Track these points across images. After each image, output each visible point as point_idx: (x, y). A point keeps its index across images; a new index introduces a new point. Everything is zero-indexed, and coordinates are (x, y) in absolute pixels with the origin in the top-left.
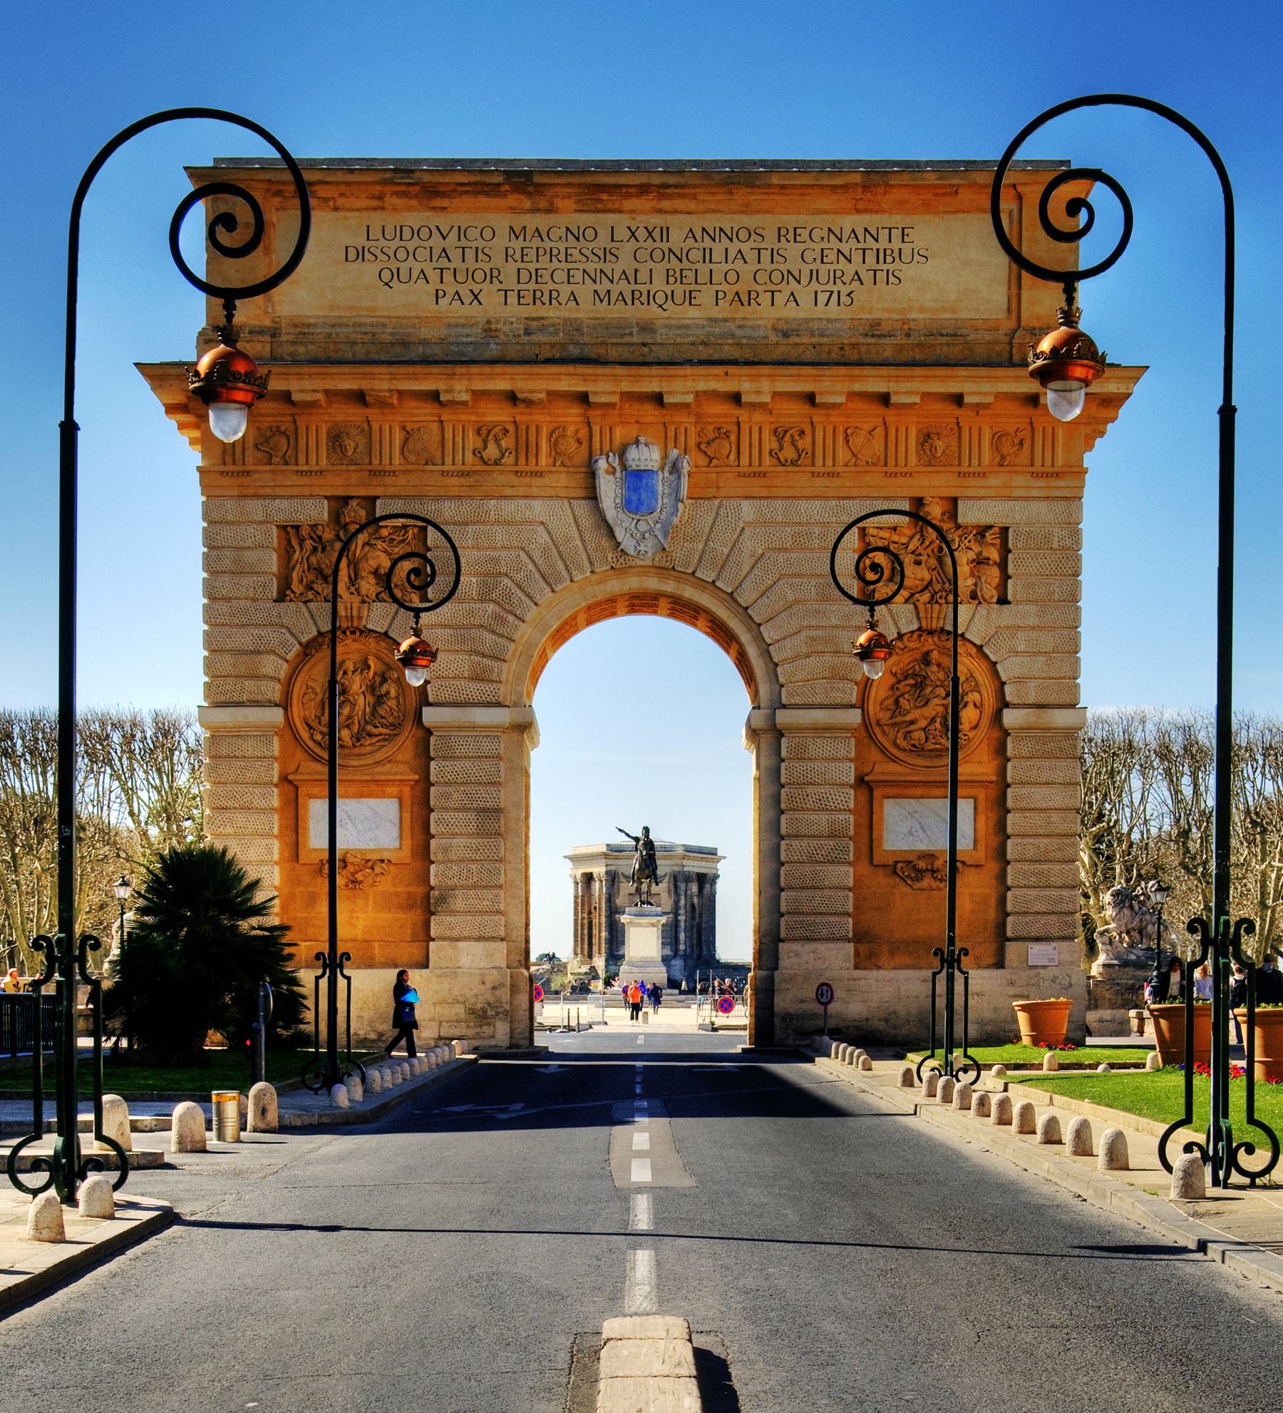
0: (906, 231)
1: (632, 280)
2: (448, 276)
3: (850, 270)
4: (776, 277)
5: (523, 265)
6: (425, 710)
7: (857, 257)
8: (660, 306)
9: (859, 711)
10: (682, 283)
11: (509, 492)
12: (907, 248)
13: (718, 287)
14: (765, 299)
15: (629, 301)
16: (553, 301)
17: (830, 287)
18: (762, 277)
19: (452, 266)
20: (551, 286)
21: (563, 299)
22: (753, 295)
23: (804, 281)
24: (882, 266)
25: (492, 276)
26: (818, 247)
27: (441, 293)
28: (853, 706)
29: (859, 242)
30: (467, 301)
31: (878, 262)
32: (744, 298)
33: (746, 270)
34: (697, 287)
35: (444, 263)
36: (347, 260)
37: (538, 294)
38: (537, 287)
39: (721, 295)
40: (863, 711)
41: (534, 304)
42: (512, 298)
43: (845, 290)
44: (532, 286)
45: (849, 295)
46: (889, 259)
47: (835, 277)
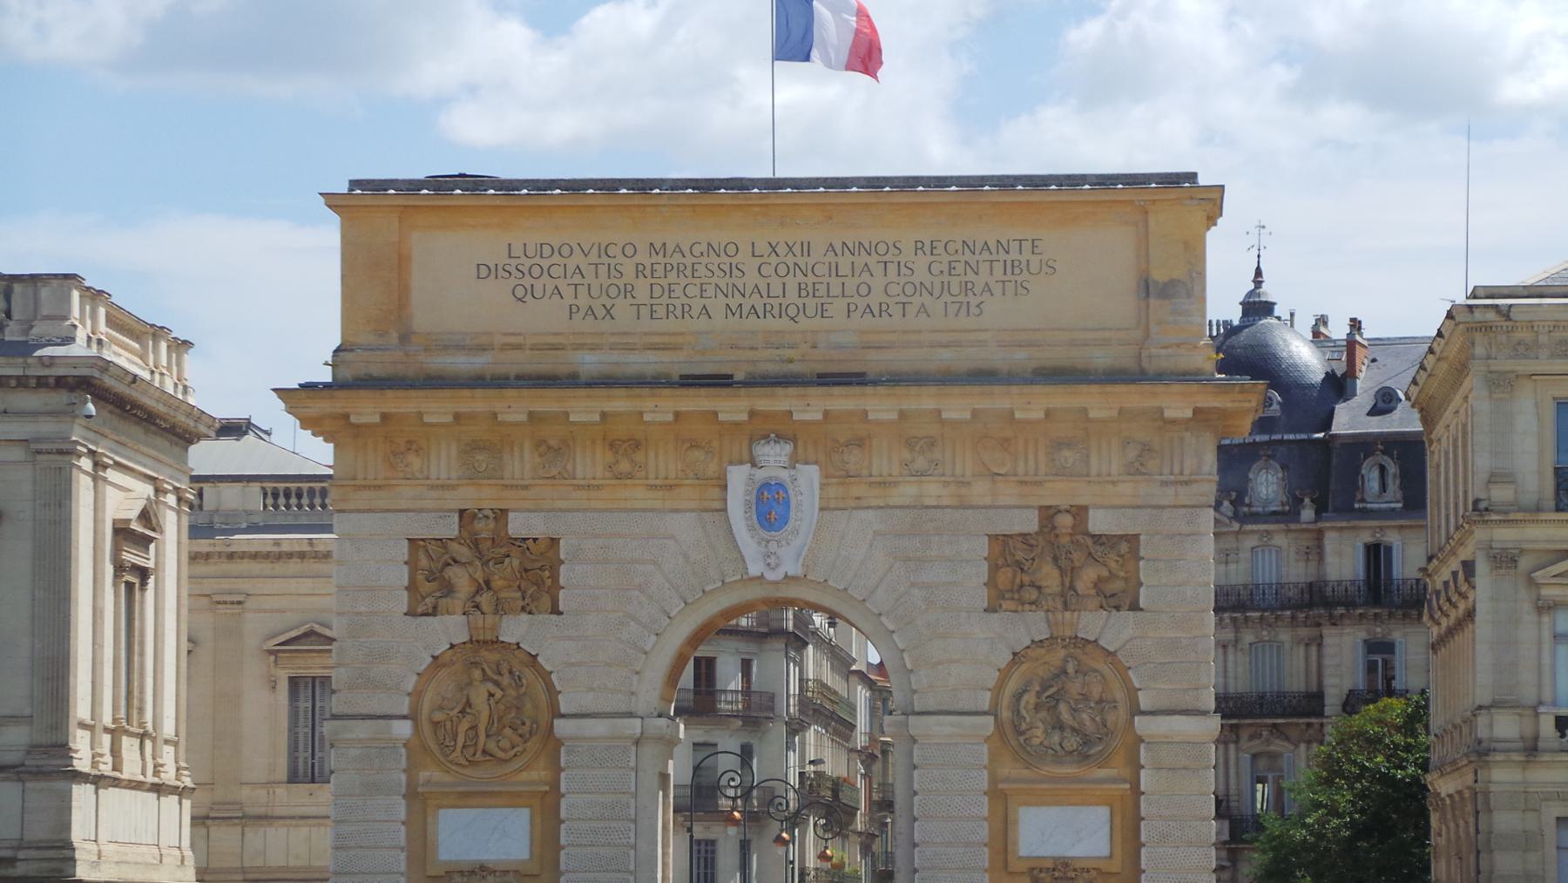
0: (1036, 243)
1: (765, 295)
2: (582, 290)
3: (980, 281)
4: (909, 290)
5: (653, 281)
6: (556, 722)
7: (984, 268)
8: (792, 318)
9: (991, 719)
10: (814, 296)
11: (639, 505)
12: (1035, 260)
13: (849, 300)
14: (896, 310)
15: (761, 315)
16: (686, 314)
17: (961, 298)
18: (894, 289)
19: (585, 282)
20: (684, 300)
21: (695, 313)
22: (884, 307)
23: (936, 293)
24: (1009, 277)
25: (628, 291)
26: (946, 258)
27: (574, 309)
28: (985, 713)
29: (991, 253)
30: (601, 312)
31: (1005, 274)
32: (876, 312)
33: (878, 282)
34: (830, 300)
35: (577, 279)
36: (478, 278)
37: (671, 308)
38: (670, 301)
39: (852, 307)
40: (996, 720)
41: (668, 318)
42: (645, 311)
43: (974, 301)
44: (665, 300)
45: (978, 306)
46: (1017, 271)
47: (966, 290)
